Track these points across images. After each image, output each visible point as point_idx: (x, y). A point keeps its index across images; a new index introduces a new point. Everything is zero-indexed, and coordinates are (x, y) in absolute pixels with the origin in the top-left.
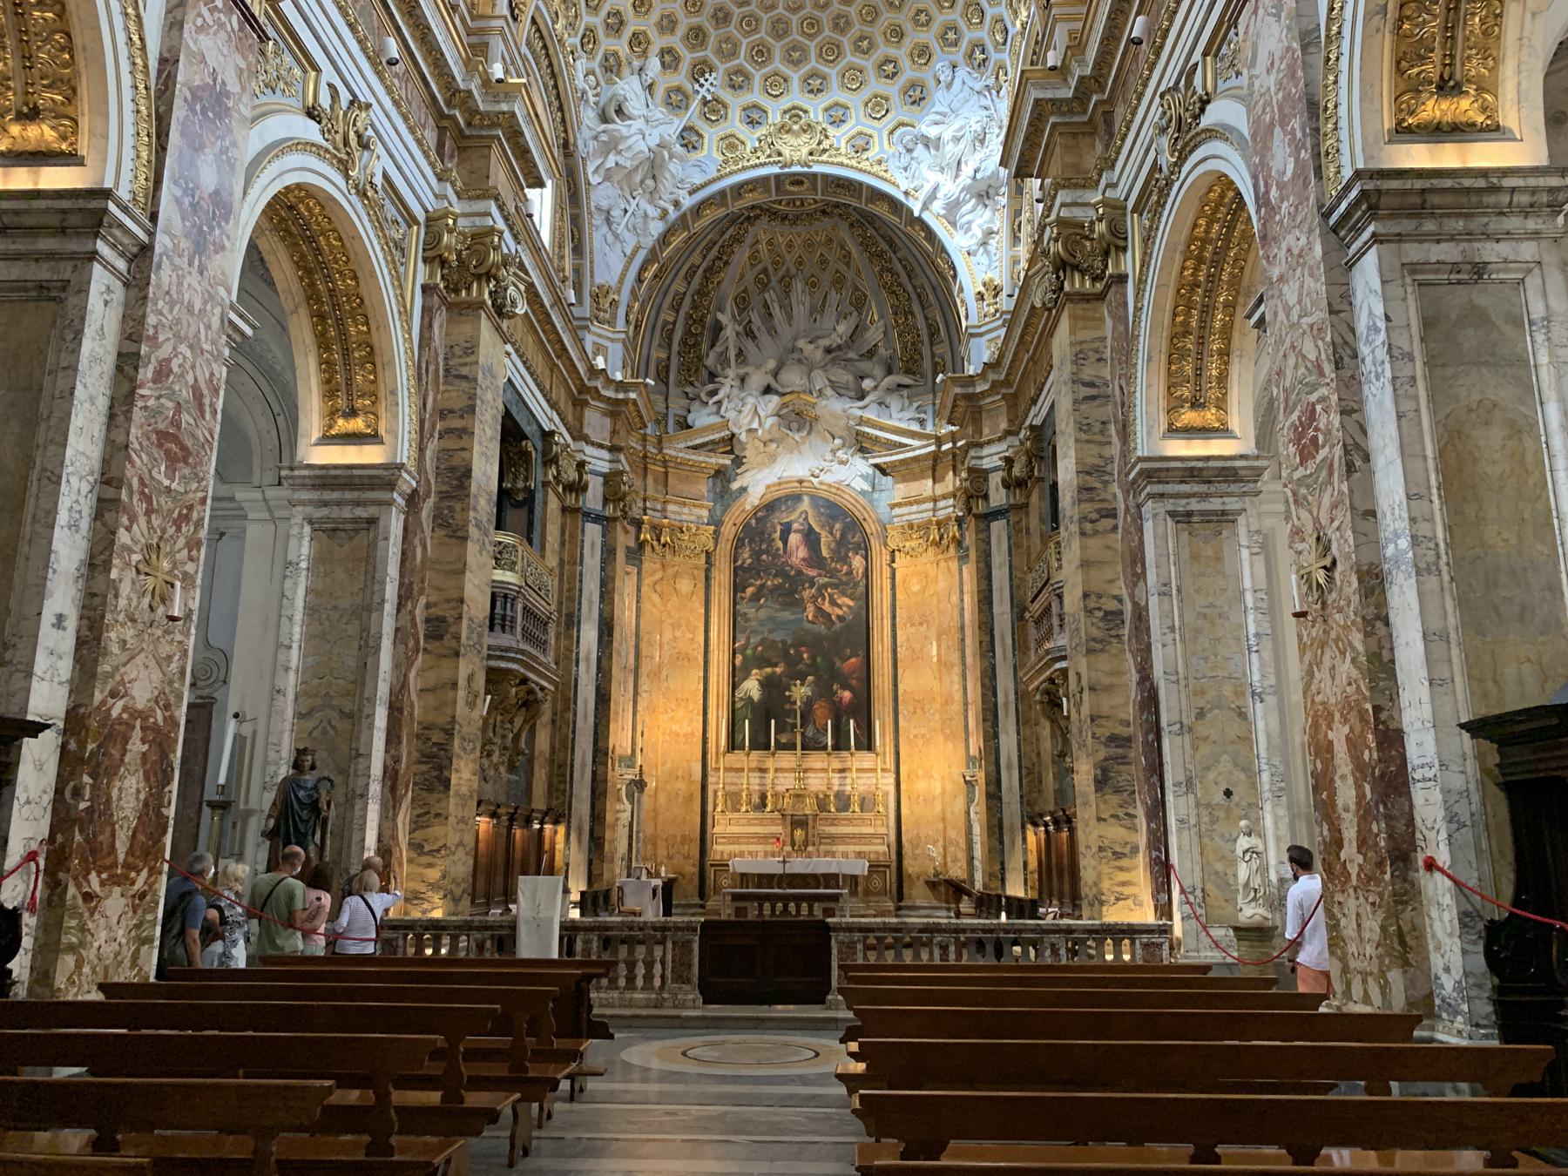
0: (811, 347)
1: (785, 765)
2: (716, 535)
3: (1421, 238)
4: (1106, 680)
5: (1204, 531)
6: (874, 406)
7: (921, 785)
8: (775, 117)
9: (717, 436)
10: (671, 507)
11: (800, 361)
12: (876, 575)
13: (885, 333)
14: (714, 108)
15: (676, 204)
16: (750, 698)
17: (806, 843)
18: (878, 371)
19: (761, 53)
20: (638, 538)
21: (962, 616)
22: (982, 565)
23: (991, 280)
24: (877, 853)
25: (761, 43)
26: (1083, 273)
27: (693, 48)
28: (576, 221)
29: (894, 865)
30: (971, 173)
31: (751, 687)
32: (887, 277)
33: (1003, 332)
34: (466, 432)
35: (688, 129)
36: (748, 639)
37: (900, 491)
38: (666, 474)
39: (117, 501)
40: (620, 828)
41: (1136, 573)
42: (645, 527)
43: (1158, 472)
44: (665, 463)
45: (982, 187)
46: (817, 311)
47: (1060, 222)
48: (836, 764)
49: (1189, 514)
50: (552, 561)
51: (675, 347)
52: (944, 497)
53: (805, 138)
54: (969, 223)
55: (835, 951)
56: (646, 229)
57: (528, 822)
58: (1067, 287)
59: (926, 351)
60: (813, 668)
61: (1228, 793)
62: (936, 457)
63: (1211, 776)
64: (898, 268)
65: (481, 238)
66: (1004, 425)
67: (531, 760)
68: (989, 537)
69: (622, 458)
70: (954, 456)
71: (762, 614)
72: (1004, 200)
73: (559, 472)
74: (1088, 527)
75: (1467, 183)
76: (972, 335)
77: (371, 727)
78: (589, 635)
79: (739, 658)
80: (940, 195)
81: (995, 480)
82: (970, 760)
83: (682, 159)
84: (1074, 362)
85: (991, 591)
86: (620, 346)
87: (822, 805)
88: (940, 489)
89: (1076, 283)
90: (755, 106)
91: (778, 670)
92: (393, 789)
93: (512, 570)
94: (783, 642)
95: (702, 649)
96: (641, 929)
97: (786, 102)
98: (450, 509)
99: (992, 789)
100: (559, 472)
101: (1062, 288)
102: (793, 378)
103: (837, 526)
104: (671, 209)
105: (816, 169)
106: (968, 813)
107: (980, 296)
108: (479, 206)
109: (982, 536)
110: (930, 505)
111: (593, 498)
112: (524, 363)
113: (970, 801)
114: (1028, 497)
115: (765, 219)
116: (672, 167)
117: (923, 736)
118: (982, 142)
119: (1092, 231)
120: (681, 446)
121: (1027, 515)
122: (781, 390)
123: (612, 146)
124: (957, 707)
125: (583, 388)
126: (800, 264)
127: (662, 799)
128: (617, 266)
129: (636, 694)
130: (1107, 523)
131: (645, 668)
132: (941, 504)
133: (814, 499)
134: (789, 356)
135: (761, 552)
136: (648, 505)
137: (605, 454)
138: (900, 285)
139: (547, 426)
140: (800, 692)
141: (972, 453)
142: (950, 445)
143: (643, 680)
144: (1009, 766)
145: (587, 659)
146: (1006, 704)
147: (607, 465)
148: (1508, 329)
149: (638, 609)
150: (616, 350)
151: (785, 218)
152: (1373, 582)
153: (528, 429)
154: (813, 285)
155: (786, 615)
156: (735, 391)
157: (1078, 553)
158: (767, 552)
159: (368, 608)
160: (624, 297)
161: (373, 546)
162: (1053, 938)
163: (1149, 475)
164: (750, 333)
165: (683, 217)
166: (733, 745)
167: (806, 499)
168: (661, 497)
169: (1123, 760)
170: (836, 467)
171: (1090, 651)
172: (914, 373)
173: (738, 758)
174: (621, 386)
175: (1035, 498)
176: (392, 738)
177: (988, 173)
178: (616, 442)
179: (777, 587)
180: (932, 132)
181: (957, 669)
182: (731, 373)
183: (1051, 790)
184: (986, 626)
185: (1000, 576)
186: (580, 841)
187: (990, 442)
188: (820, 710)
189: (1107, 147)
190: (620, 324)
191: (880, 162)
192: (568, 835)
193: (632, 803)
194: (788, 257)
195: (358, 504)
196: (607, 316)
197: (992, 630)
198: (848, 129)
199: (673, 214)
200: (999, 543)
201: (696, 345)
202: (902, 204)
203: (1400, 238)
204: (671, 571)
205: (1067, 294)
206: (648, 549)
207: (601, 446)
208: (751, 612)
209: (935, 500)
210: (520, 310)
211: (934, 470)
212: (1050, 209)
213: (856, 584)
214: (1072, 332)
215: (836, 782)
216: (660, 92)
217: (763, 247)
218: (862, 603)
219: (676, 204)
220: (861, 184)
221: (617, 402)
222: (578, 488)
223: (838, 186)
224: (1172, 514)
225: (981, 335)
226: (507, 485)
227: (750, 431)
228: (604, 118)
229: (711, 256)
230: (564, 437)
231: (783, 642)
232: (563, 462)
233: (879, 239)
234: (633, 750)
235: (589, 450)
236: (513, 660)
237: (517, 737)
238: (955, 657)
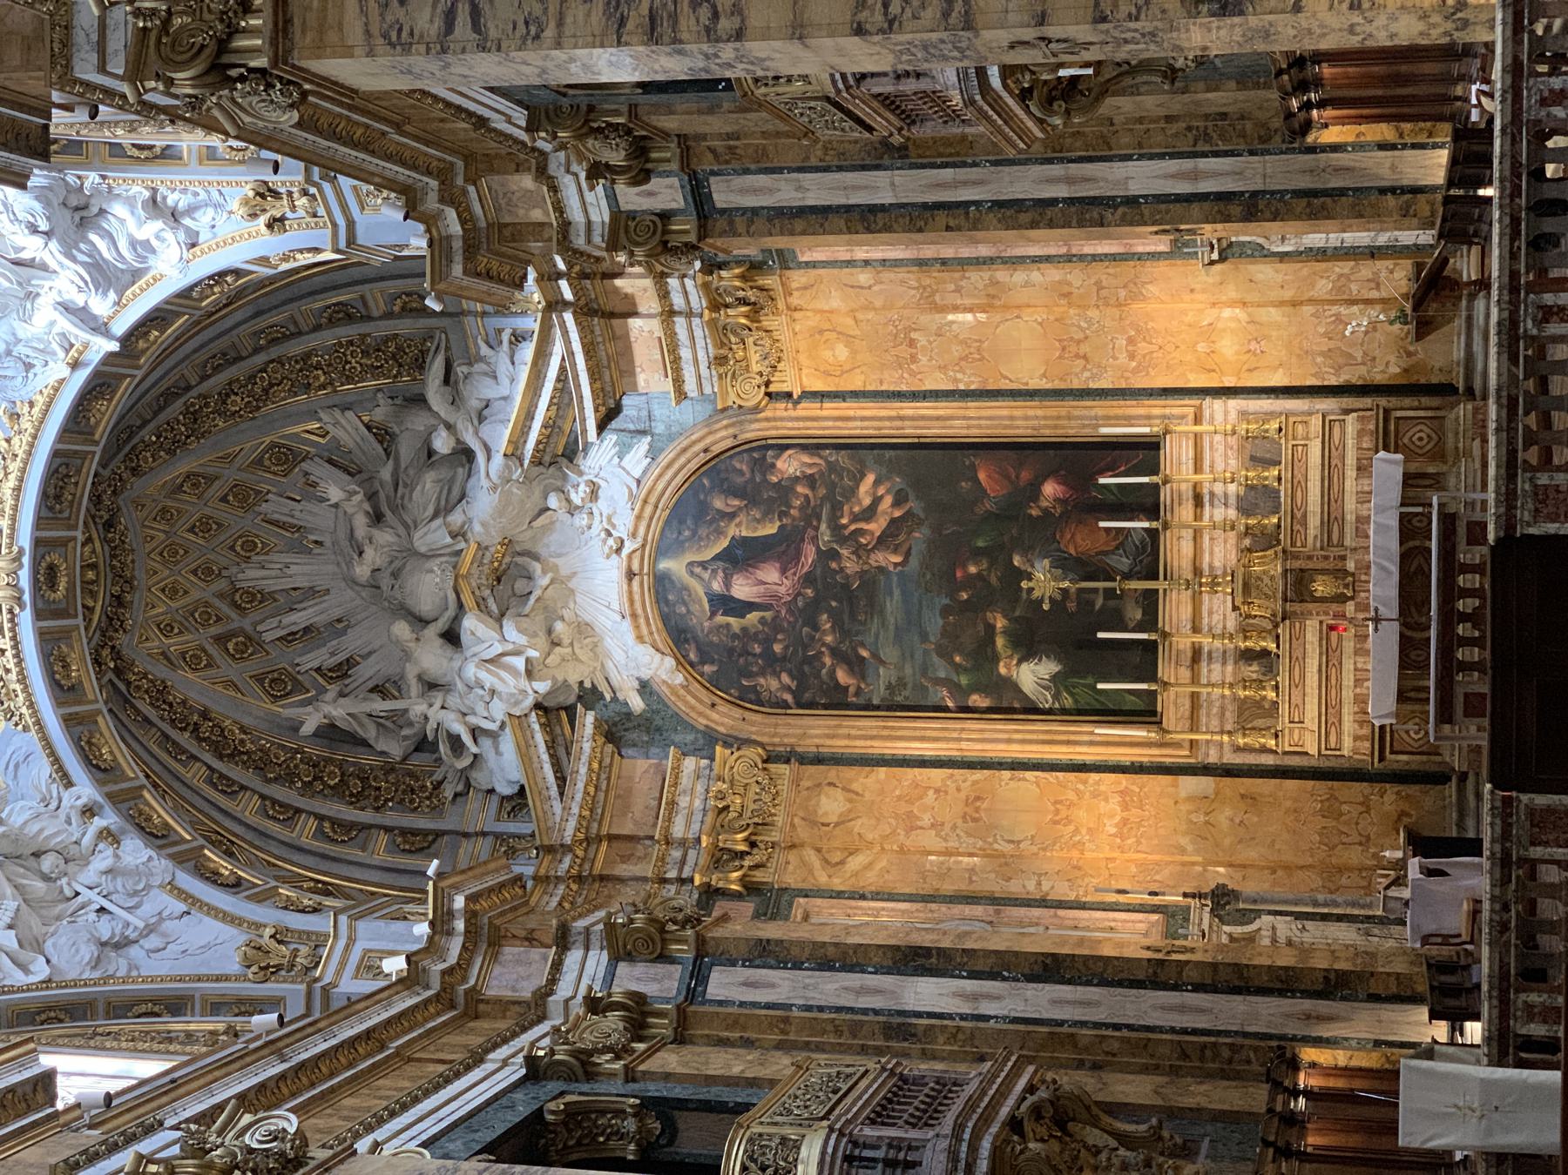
0: (369, 553)
1: (1186, 612)
2: (735, 742)
6: (486, 430)
7: (1228, 347)
9: (540, 738)
10: (678, 830)
11: (395, 575)
12: (815, 429)
13: (345, 408)
15: (89, 812)
16: (1055, 678)
18: (417, 422)
20: (737, 896)
22: (799, 224)
23: (245, 202)
24: (1360, 434)
26: (234, 31)
28: (121, 1007)
29: (1383, 402)
30: (38, 241)
31: (1032, 676)
33: (345, 182)
36: (938, 682)
37: (650, 378)
38: (612, 838)
40: (1307, 938)
42: (716, 880)
44: (590, 841)
45: (66, 219)
46: (299, 539)
47: (135, 73)
48: (1186, 512)
50: (780, 1065)
51: (367, 816)
52: (664, 295)
54: (133, 243)
55: (1552, 528)
56: (135, 872)
57: (1292, 1121)
58: (261, 62)
59: (380, 329)
60: (997, 554)
62: (587, 311)
66: (527, 181)
67: (1172, 1113)
68: (744, 211)
69: (580, 924)
70: (584, 276)
71: (890, 653)
72: (92, 178)
73: (607, 1049)
74: (725, 25)
76: (351, 240)
79: (976, 700)
80: (80, 300)
81: (632, 198)
82: (1179, 251)
84: (407, 49)
85: (848, 208)
86: (361, 925)
87: (1262, 540)
88: (648, 302)
89: (253, 46)
91: (1000, 623)
93: (797, 1146)
94: (945, 611)
95: (958, 773)
96: (1506, 908)
99: (1236, 210)
100: (607, 1049)
101: (262, 72)
103: (718, 503)
104: (98, 823)
105: (25, 539)
106: (1283, 257)
107: (276, 224)
110: (680, 323)
112: (393, 1114)
114: (666, 135)
115: (121, 640)
117: (1131, 341)
119: (153, 12)
120: (557, 807)
121: (704, 137)
122: (451, 613)
124: (1075, 276)
125: (445, 999)
126: (209, 571)
127: (1251, 854)
128: (206, 930)
129: (1043, 903)
131: (991, 884)
132: (678, 301)
135: (768, 655)
136: (672, 874)
137: (573, 957)
138: (252, 378)
139: (517, 1071)
140: (1043, 581)
141: (580, 242)
142: (564, 284)
143: (1015, 888)
144: (1195, 176)
145: (975, 997)
146: (1070, 181)
147: (593, 954)
149: (877, 896)
150: (372, 933)
151: (119, 600)
153: (522, 1108)
154: (249, 548)
155: (893, 605)
156: (453, 700)
157: (777, 44)
158: (767, 642)
160: (268, 915)
162: (1529, 100)
164: (341, 671)
165: (113, 798)
166: (1145, 713)
167: (664, 565)
168: (656, 850)
170: (602, 506)
171: (968, 24)
172: (424, 353)
173: (1173, 706)
174: (441, 925)
175: (669, 123)
177: (38, 206)
178: (548, 939)
179: (838, 625)
181: (1002, 275)
182: (417, 708)
183: (1241, 95)
185: (818, 190)
186: (1330, 1019)
187: (559, 208)
188: (1078, 542)
190: (320, 924)
191: (15, 416)
192: (1318, 1042)
193: (1258, 913)
194: (195, 595)
196: (304, 950)
197: (925, 206)
199: (109, 819)
200: (756, 191)
202: (96, 374)
204: (803, 833)
205: (275, 62)
206: (759, 876)
207: (557, 966)
208: (885, 675)
209: (669, 314)
210: (291, 1124)
211: (612, 315)
212: (109, 93)
213: (832, 467)
214: (348, 52)
217: (174, 644)
218: (869, 456)
219: (89, 812)
220: (55, 454)
221: (471, 933)
222: (638, 1011)
223: (58, 497)
225: (351, 224)
226: (630, 1152)
227: (530, 674)
229: (193, 748)
230: (537, 1038)
231: (945, 611)
232: (588, 1040)
233: (162, 417)
234: (1155, 909)
235: (564, 989)
236: (974, 1148)
237: (1124, 1140)
238: (977, 278)
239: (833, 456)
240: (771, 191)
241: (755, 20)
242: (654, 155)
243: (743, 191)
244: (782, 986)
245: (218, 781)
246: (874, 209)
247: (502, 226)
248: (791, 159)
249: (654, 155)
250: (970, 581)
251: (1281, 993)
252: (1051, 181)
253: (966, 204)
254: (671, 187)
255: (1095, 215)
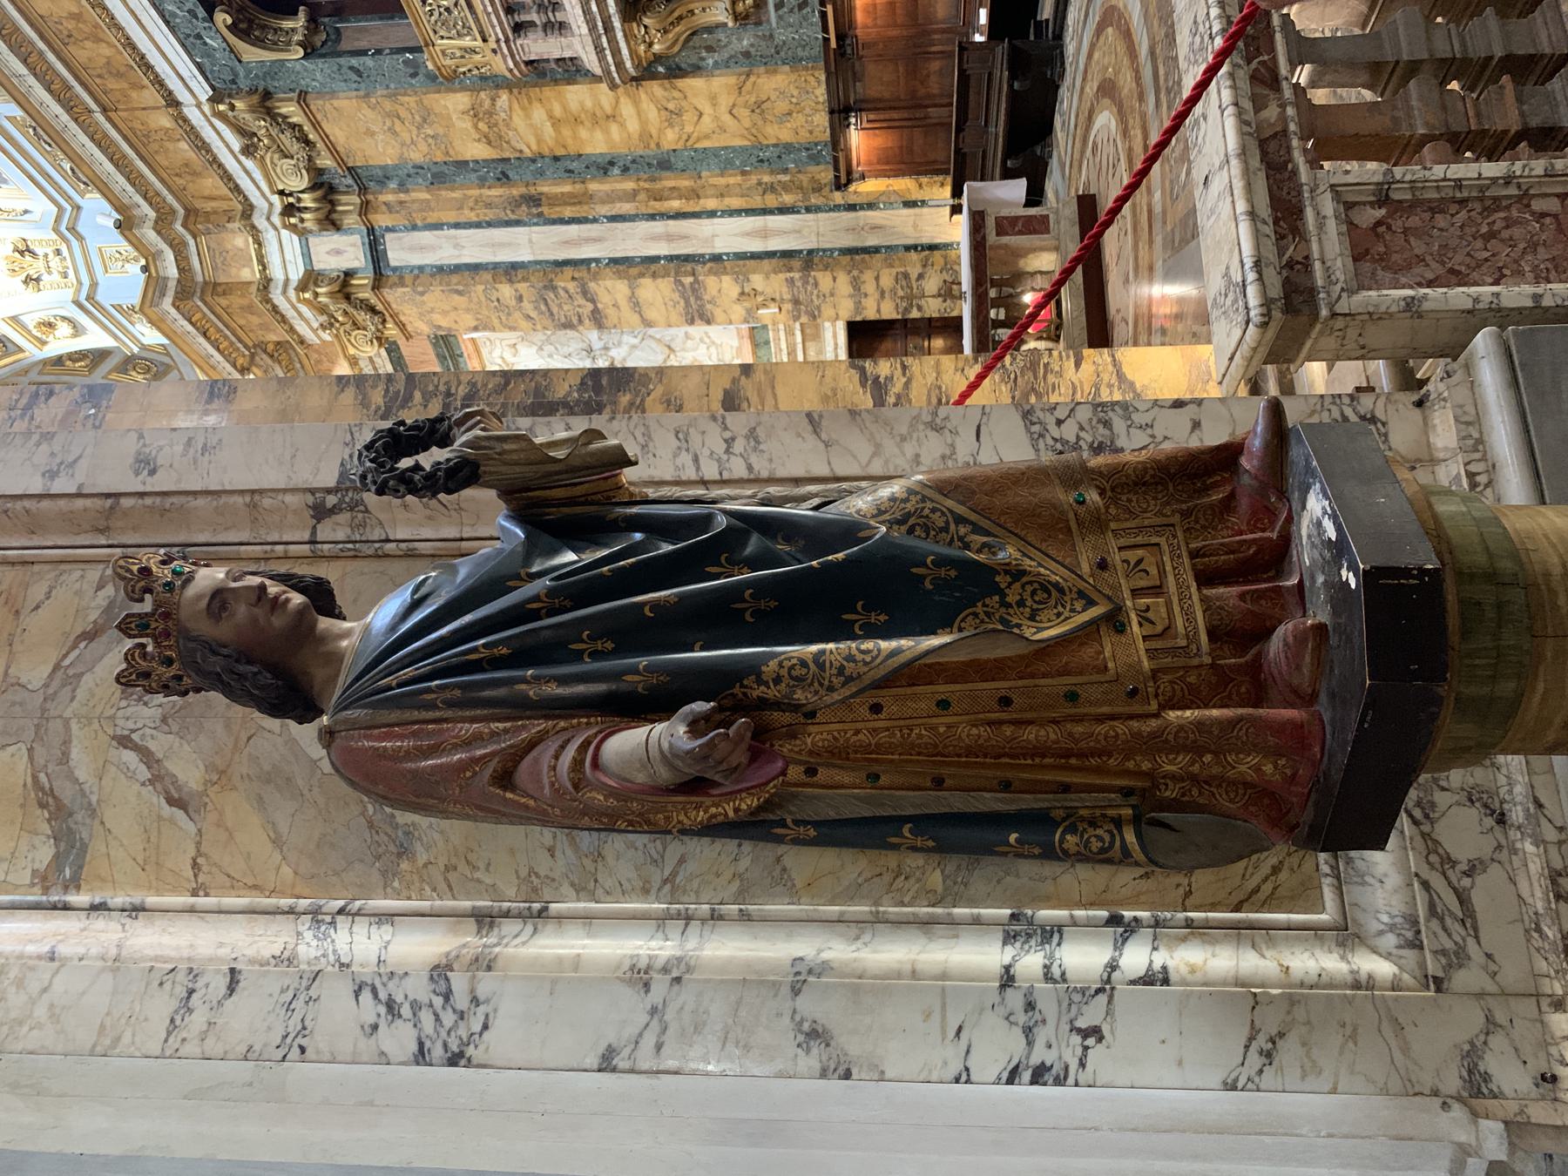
66: (240, 240)
85: (496, 266)
99: (796, 263)
109: (408, 279)
144: (764, 234)
146: (670, 238)
187: (264, 266)
225: (94, 285)
240: (432, 248)
242: (340, 208)
243: (412, 249)
246: (514, 266)
247: (216, 285)
249: (340, 208)
252: (656, 238)
253: (586, 262)
254: (354, 245)
255: (689, 268)
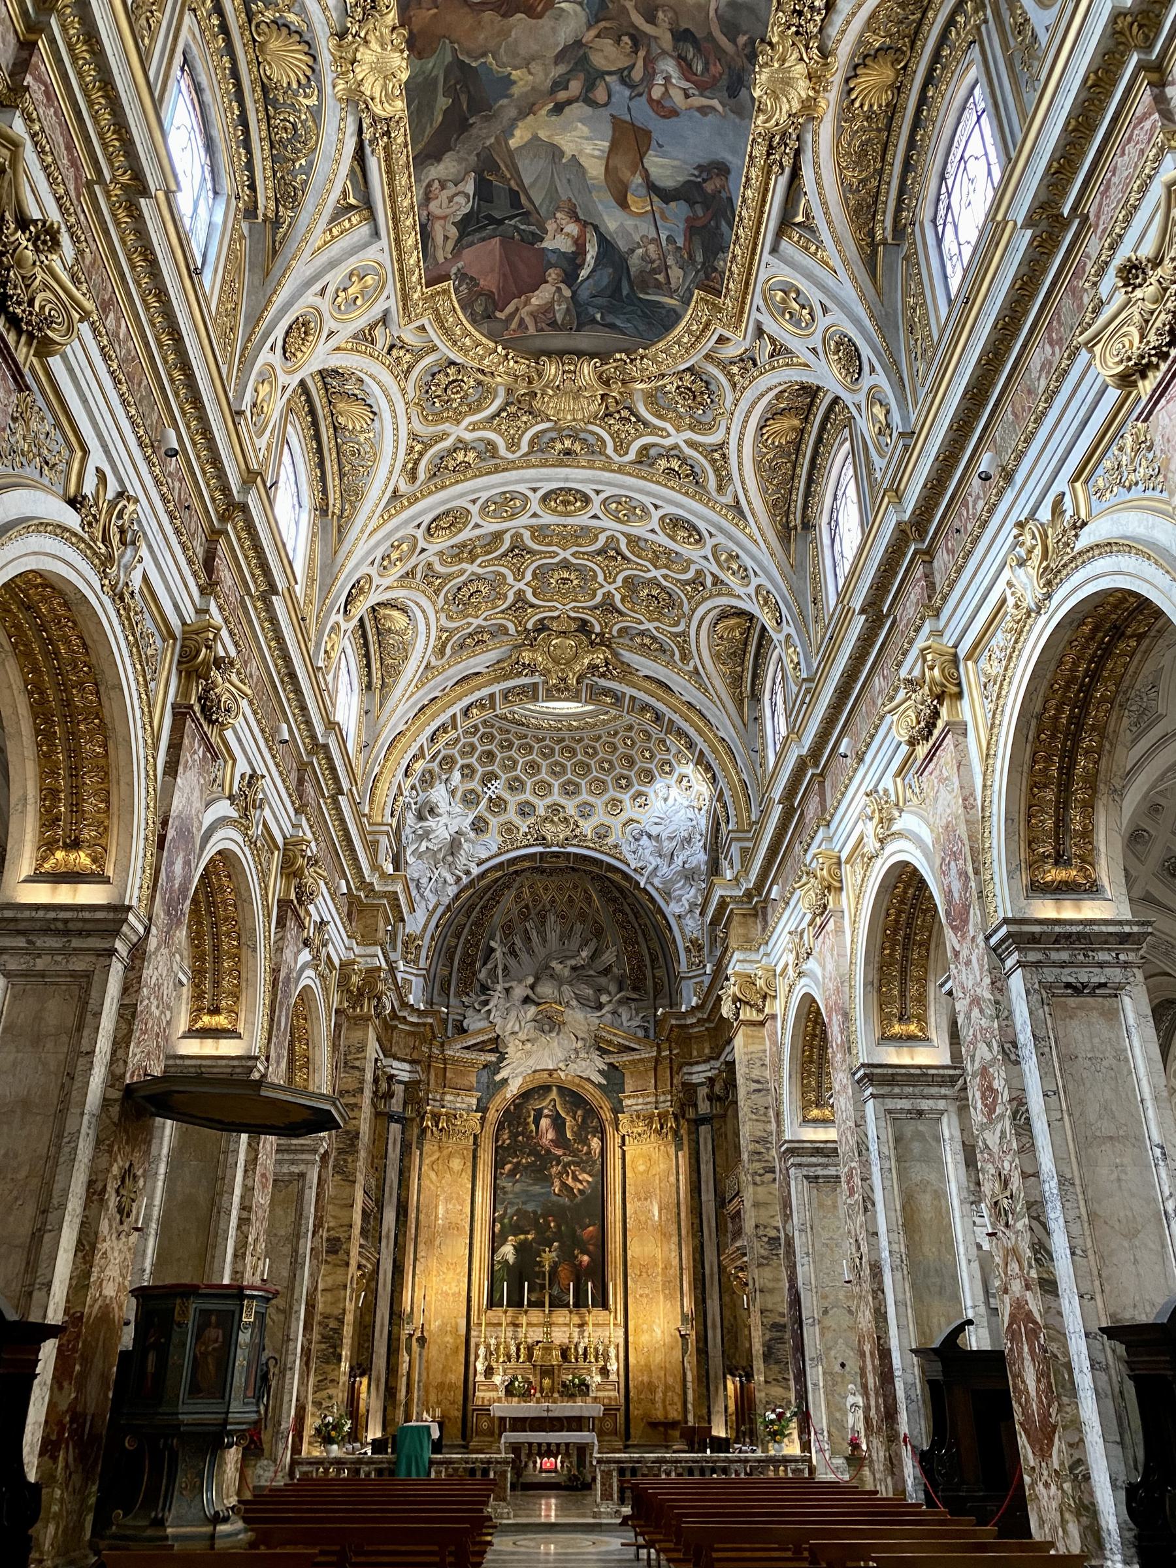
0: (561, 966)
1: (534, 1320)
3: (894, 1096)
4: (770, 1285)
5: (826, 1188)
7: (644, 1338)
8: (541, 811)
9: (486, 1038)
10: (448, 1097)
12: (610, 1155)
14: (497, 804)
17: (552, 1390)
18: (613, 988)
19: (533, 766)
21: (678, 1193)
25: (534, 761)
27: (483, 765)
31: (508, 1251)
32: (620, 916)
34: (356, 1107)
35: (479, 818)
39: (249, 1219)
41: (788, 1217)
43: (796, 1150)
45: (689, 873)
49: (817, 1177)
53: (562, 826)
58: (741, 1017)
60: (558, 1236)
61: (843, 1365)
62: (657, 1060)
63: (833, 1353)
64: (628, 910)
65: (372, 973)
71: (518, 1187)
74: (758, 1179)
75: (912, 1071)
77: (298, 1319)
78: (390, 1216)
79: (498, 1226)
81: (703, 1091)
82: (685, 1318)
83: (472, 842)
90: (528, 803)
92: (307, 1364)
94: (535, 1212)
97: (548, 801)
98: (345, 1161)
99: (701, 1345)
102: (546, 989)
107: (688, 950)
108: (371, 950)
111: (396, 1105)
113: (684, 1352)
114: (726, 1111)
116: (465, 846)
118: (689, 842)
123: (426, 835)
124: (674, 1271)
129: (415, 1259)
130: (769, 1176)
132: (662, 1098)
133: (561, 1089)
134: (543, 973)
137: (407, 1066)
140: (549, 1257)
141: (685, 1070)
143: (421, 1247)
145: (388, 1237)
146: (712, 1275)
148: (934, 1144)
151: (543, 871)
152: (876, 1270)
155: (537, 1189)
158: (522, 1134)
159: (297, 1236)
161: (301, 1194)
163: (792, 1151)
164: (513, 953)
166: (492, 1304)
169: (781, 1340)
171: (760, 1265)
173: (497, 1314)
176: (308, 1327)
179: (529, 1165)
180: (654, 831)
181: (675, 1239)
182: (499, 987)
184: (696, 1210)
185: (706, 1169)
187: (697, 1063)
188: (564, 1272)
189: (764, 929)
190: (422, 963)
191: (616, 846)
193: (410, 1355)
195: (293, 1162)
198: (594, 821)
199: (465, 880)
201: (473, 964)
203: (883, 1096)
204: (446, 1152)
207: (404, 1060)
211: (655, 1070)
214: (746, 1046)
215: (576, 1335)
216: (459, 794)
217: (526, 890)
219: (468, 873)
222: (389, 1095)
224: (807, 1177)
228: (420, 817)
231: (535, 1212)
235: (396, 1064)
239: (599, 1162)
241: (759, 1189)
244: (394, 1154)
245: (472, 908)
248: (719, 1161)
250: (548, 1223)
251: (388, 1368)
